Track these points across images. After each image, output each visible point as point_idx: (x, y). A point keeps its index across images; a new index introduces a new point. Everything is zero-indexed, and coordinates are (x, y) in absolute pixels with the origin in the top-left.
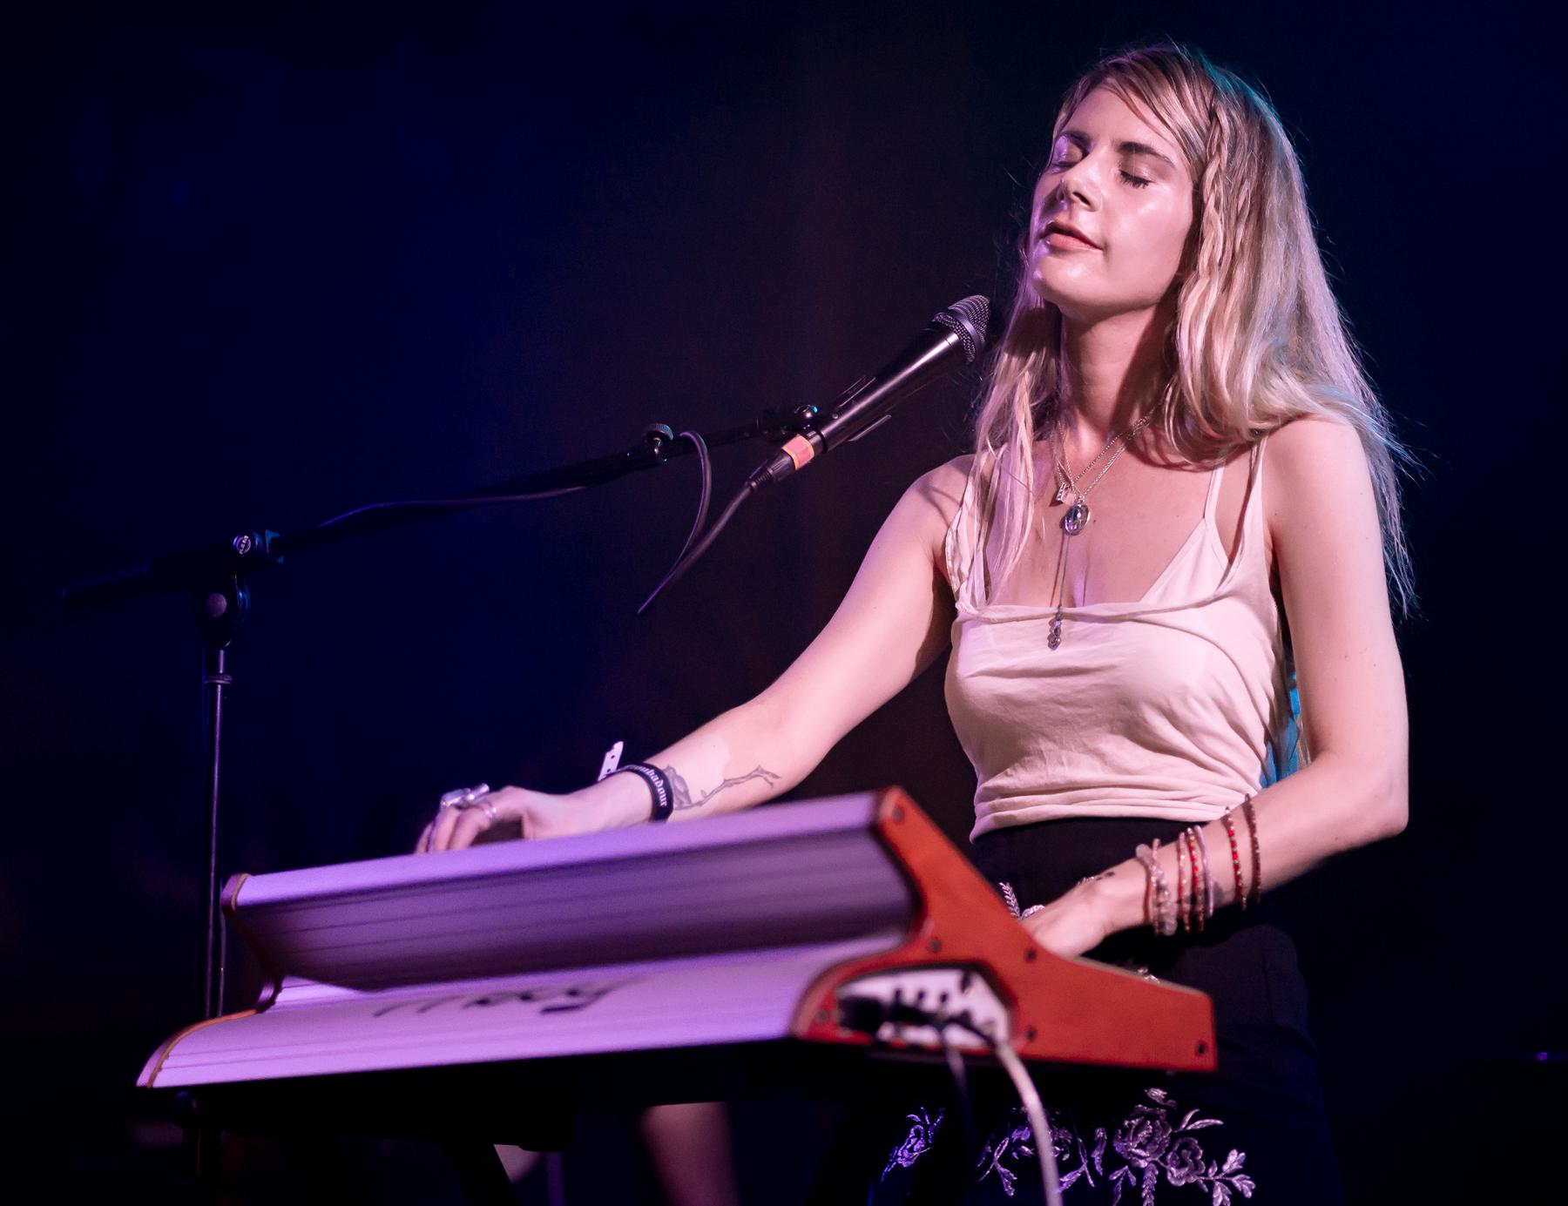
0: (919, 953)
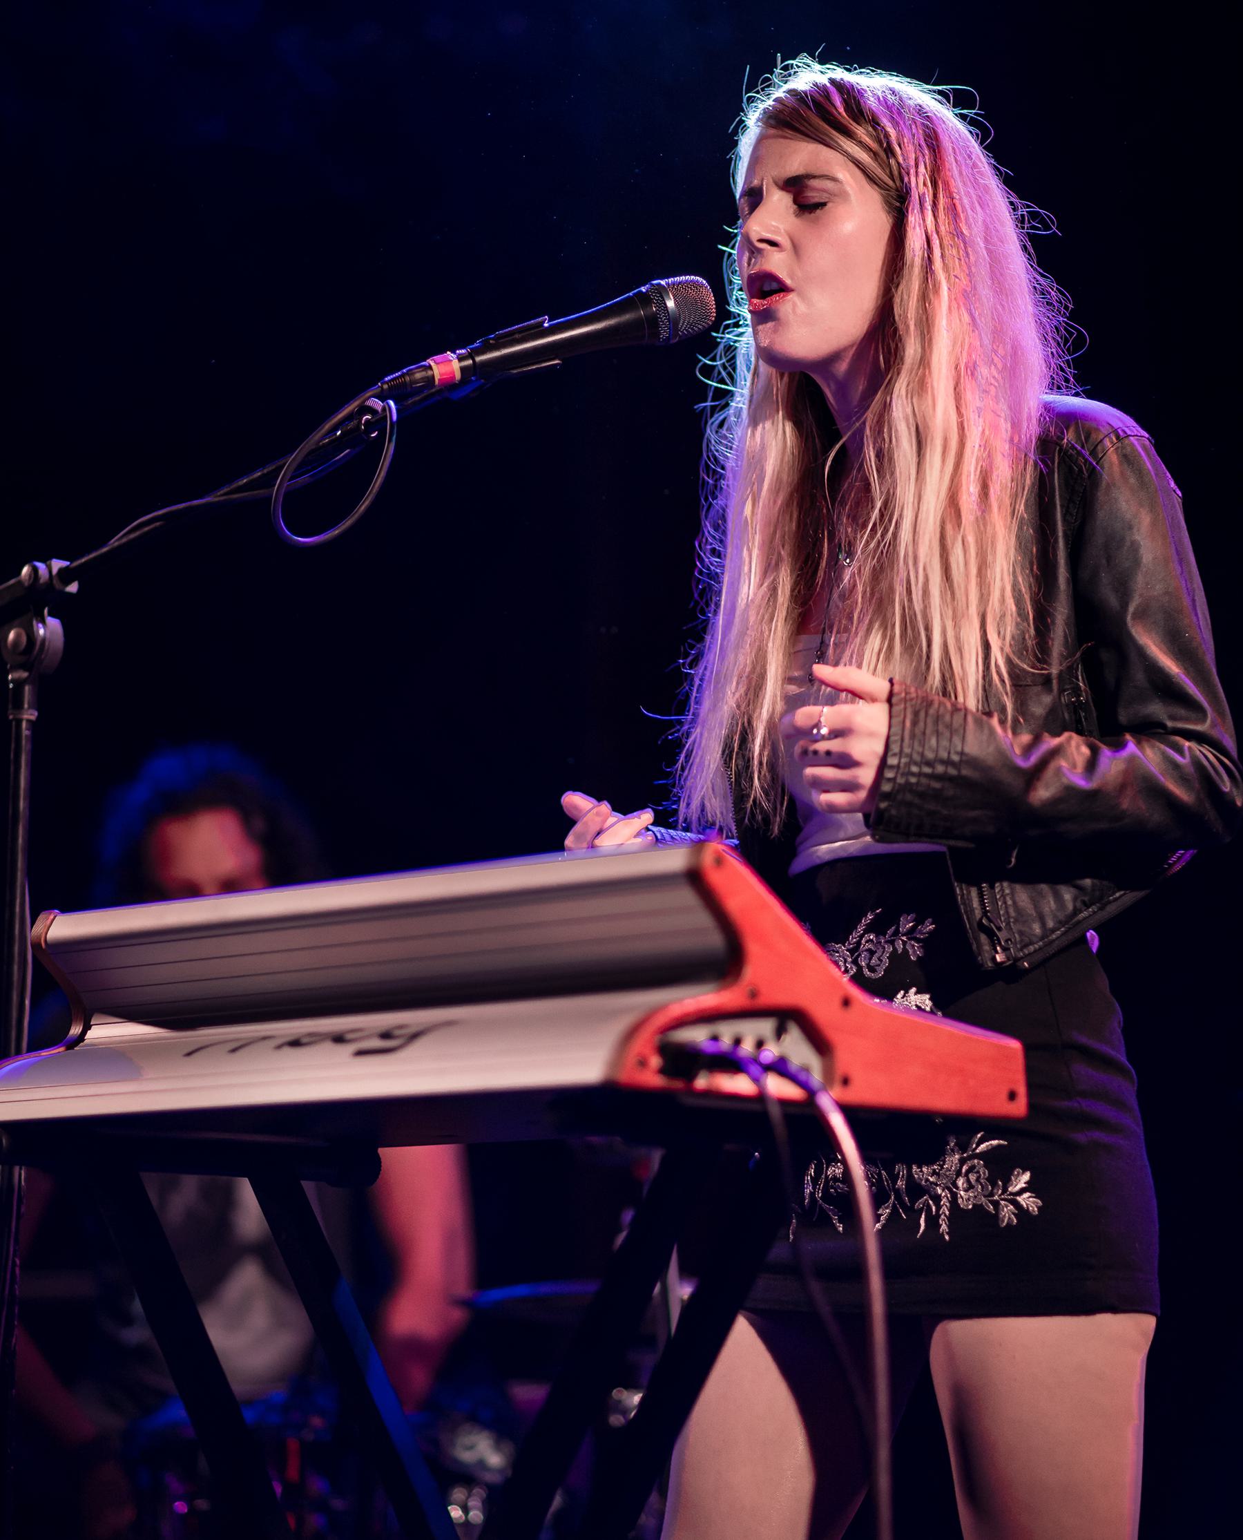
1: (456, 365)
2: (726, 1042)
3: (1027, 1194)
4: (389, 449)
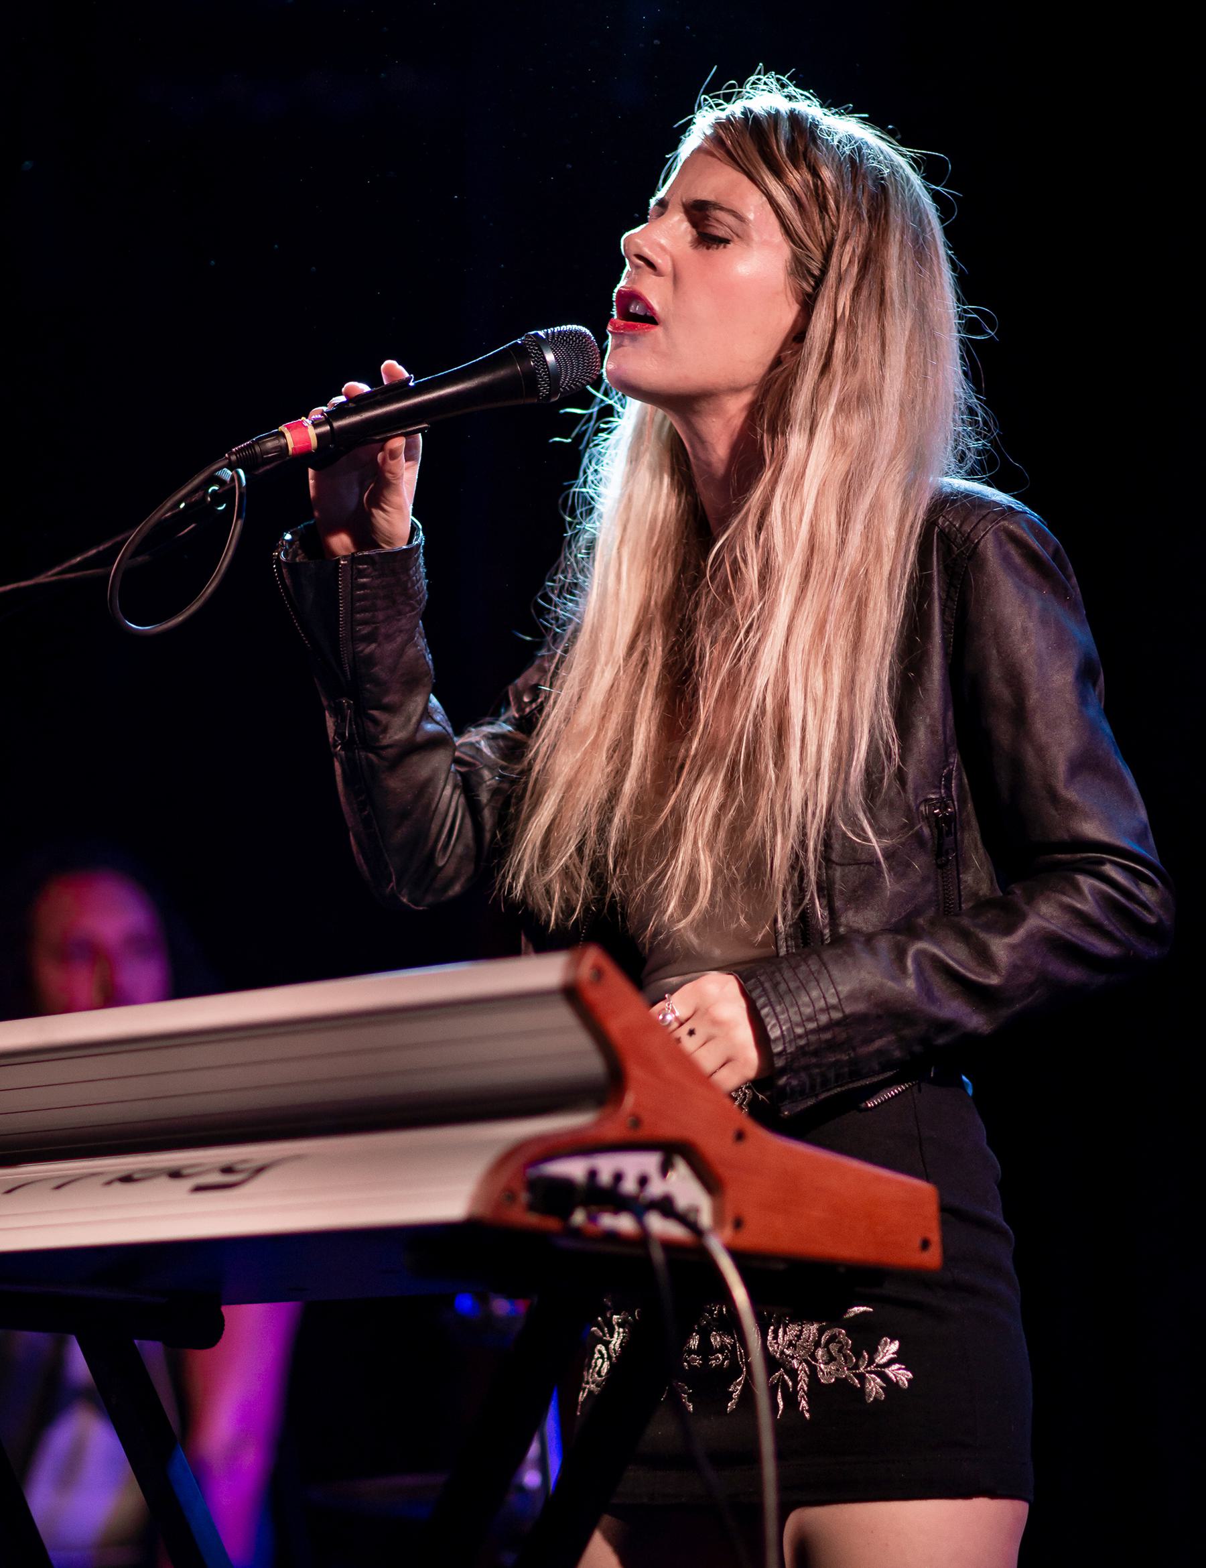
0: (614, 1130)
1: (312, 433)
2: (605, 1178)
3: (897, 1366)
4: (237, 527)
